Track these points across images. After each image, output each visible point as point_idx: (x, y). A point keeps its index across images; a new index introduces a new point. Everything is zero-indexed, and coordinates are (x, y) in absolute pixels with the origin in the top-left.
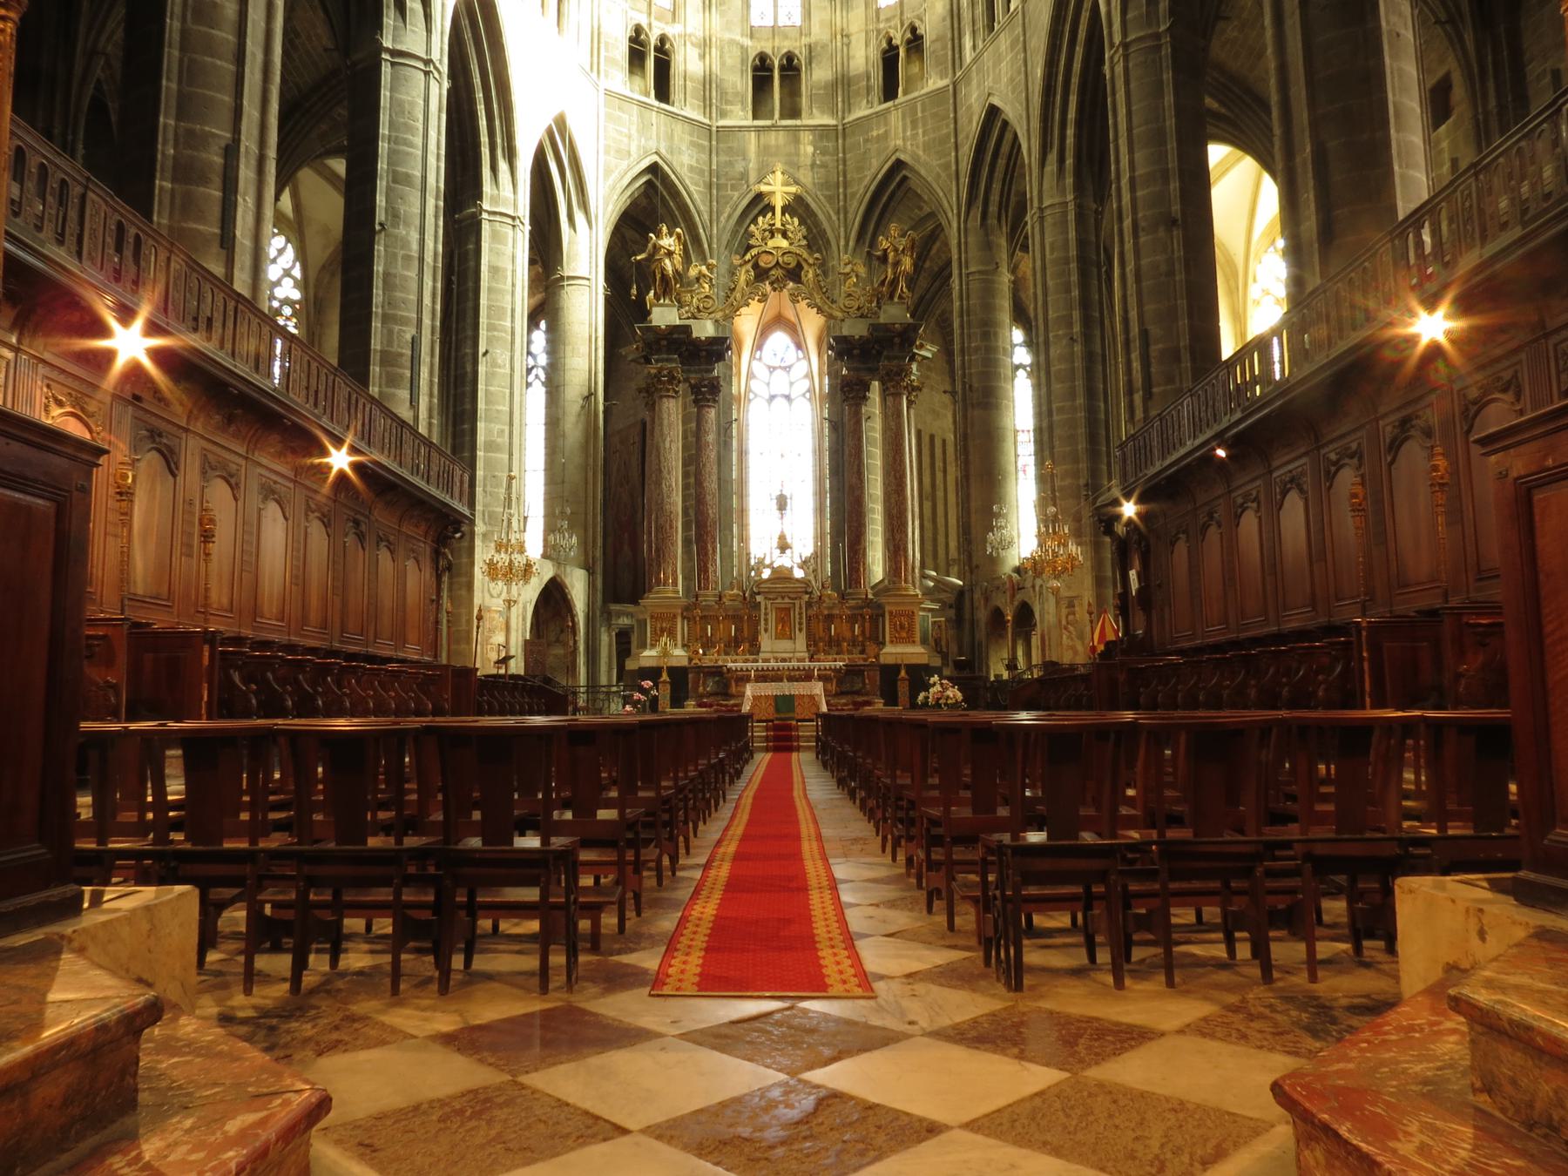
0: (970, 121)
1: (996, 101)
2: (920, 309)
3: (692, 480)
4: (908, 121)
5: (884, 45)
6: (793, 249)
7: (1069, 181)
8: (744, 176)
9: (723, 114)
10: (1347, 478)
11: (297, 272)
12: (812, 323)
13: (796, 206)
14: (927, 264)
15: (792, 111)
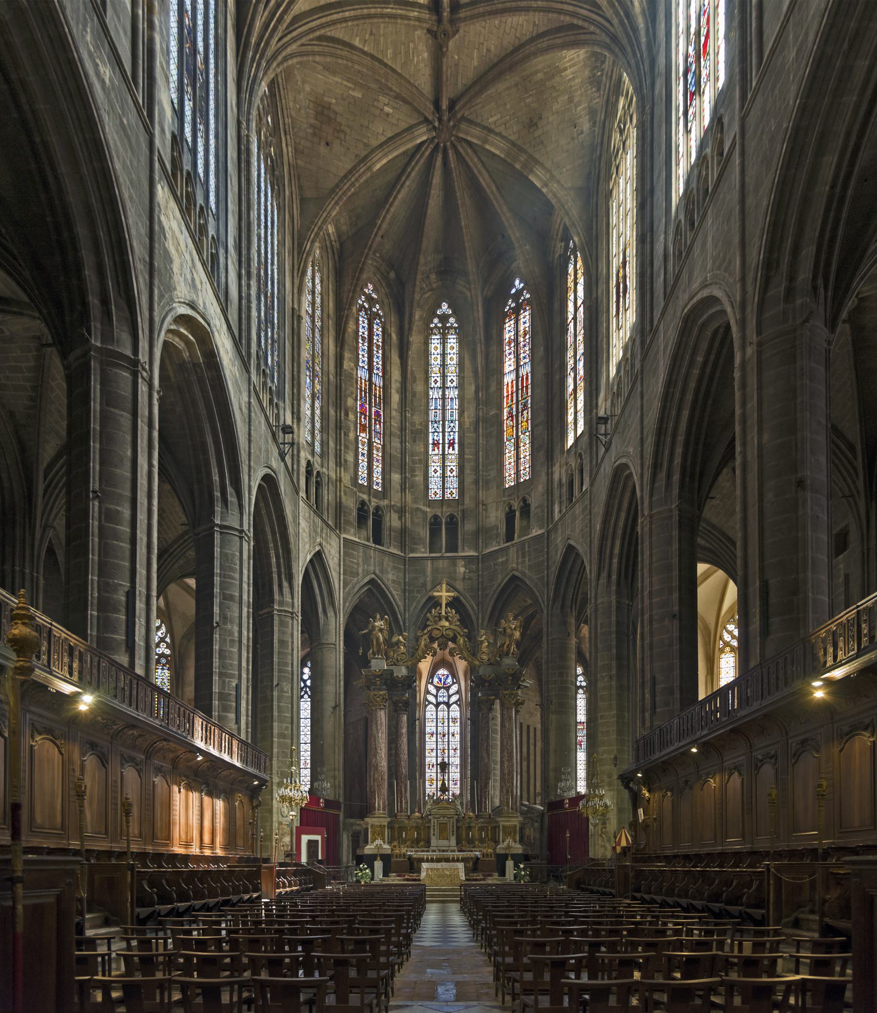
0: (556, 554)
1: (572, 542)
2: (522, 660)
3: (394, 752)
4: (520, 553)
5: (507, 509)
6: (452, 627)
7: (614, 588)
8: (424, 585)
9: (413, 551)
10: (768, 770)
11: (168, 640)
12: (461, 665)
13: (454, 603)
14: (529, 632)
15: (452, 547)
